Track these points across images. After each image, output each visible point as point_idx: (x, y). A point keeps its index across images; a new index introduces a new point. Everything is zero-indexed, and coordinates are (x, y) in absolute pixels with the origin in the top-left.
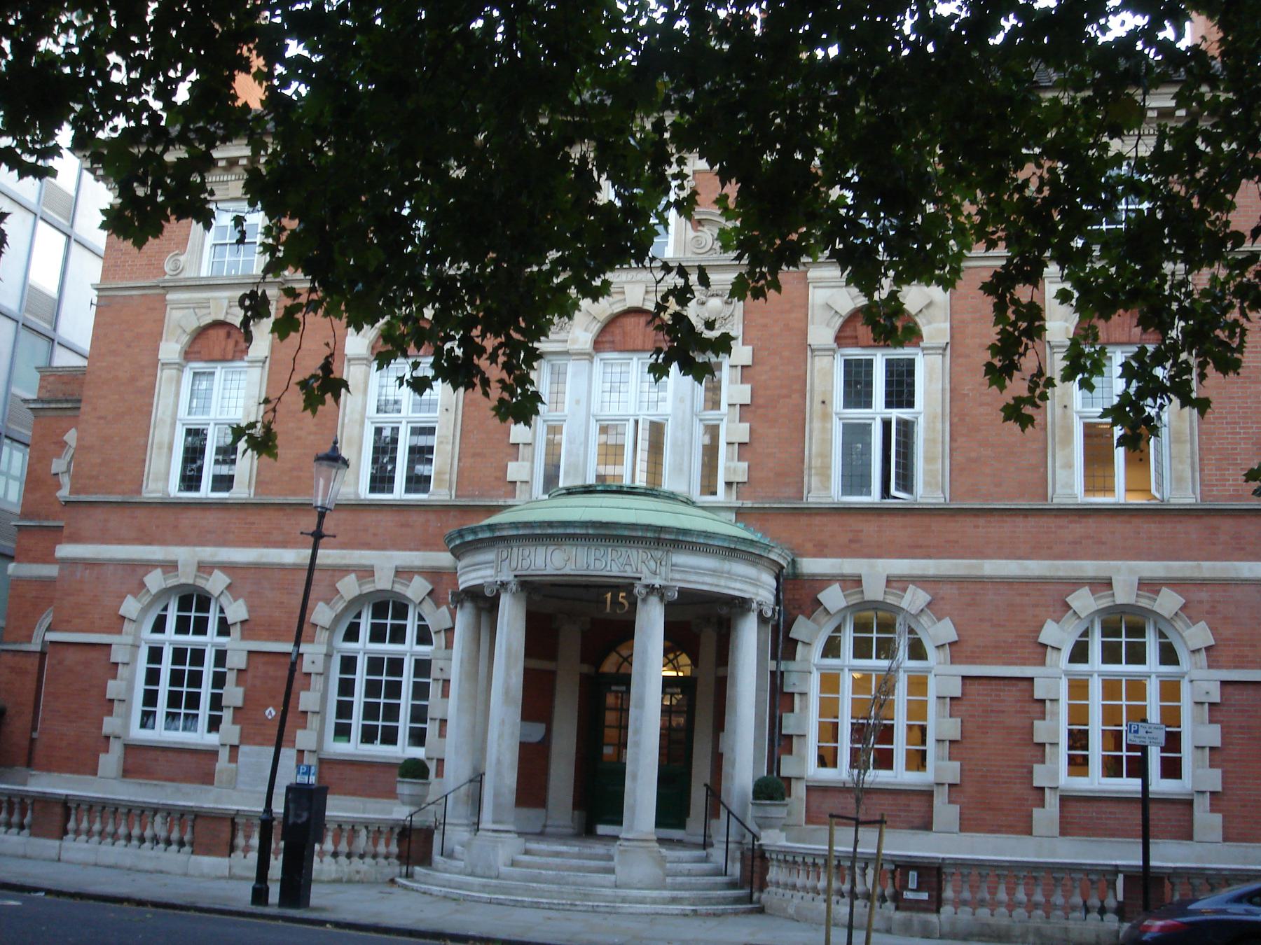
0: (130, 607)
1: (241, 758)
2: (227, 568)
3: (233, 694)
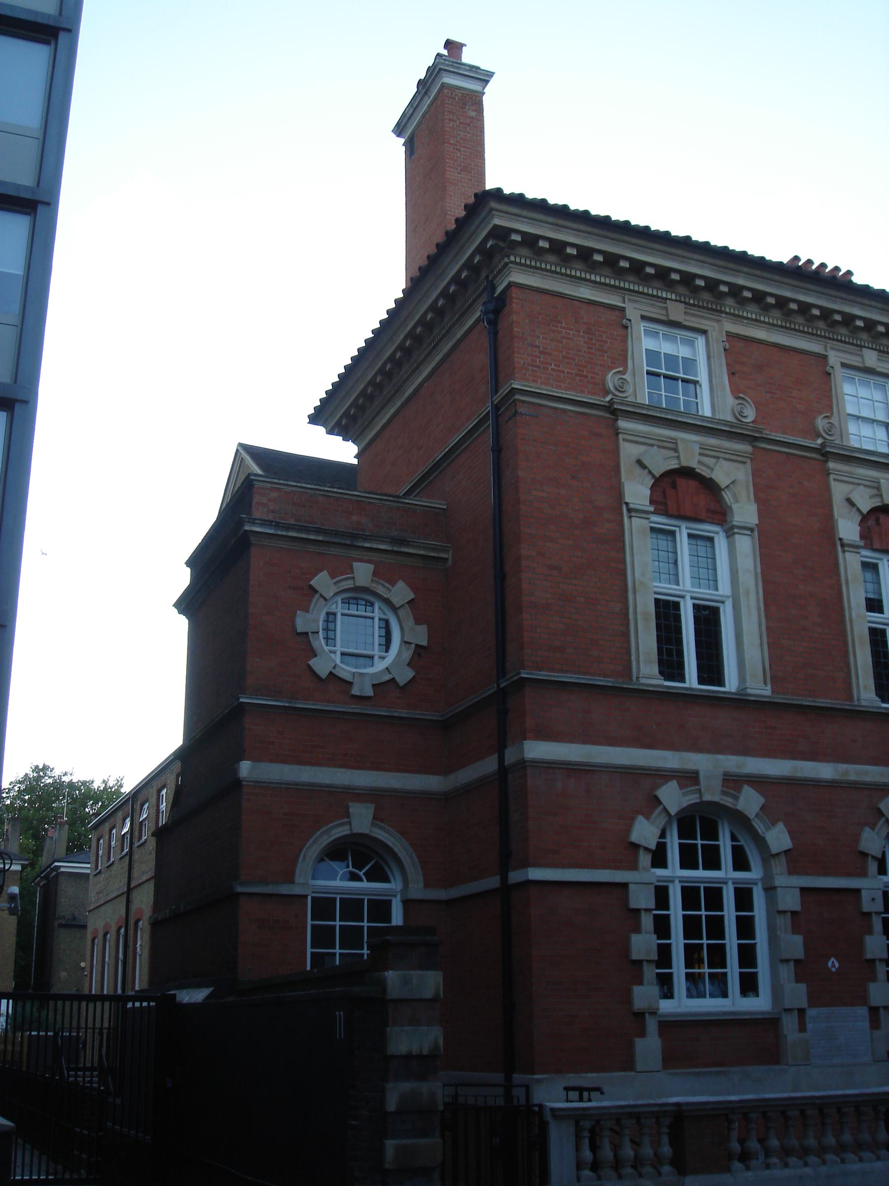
0: (645, 832)
1: (809, 1026)
2: (759, 782)
3: (643, 944)
